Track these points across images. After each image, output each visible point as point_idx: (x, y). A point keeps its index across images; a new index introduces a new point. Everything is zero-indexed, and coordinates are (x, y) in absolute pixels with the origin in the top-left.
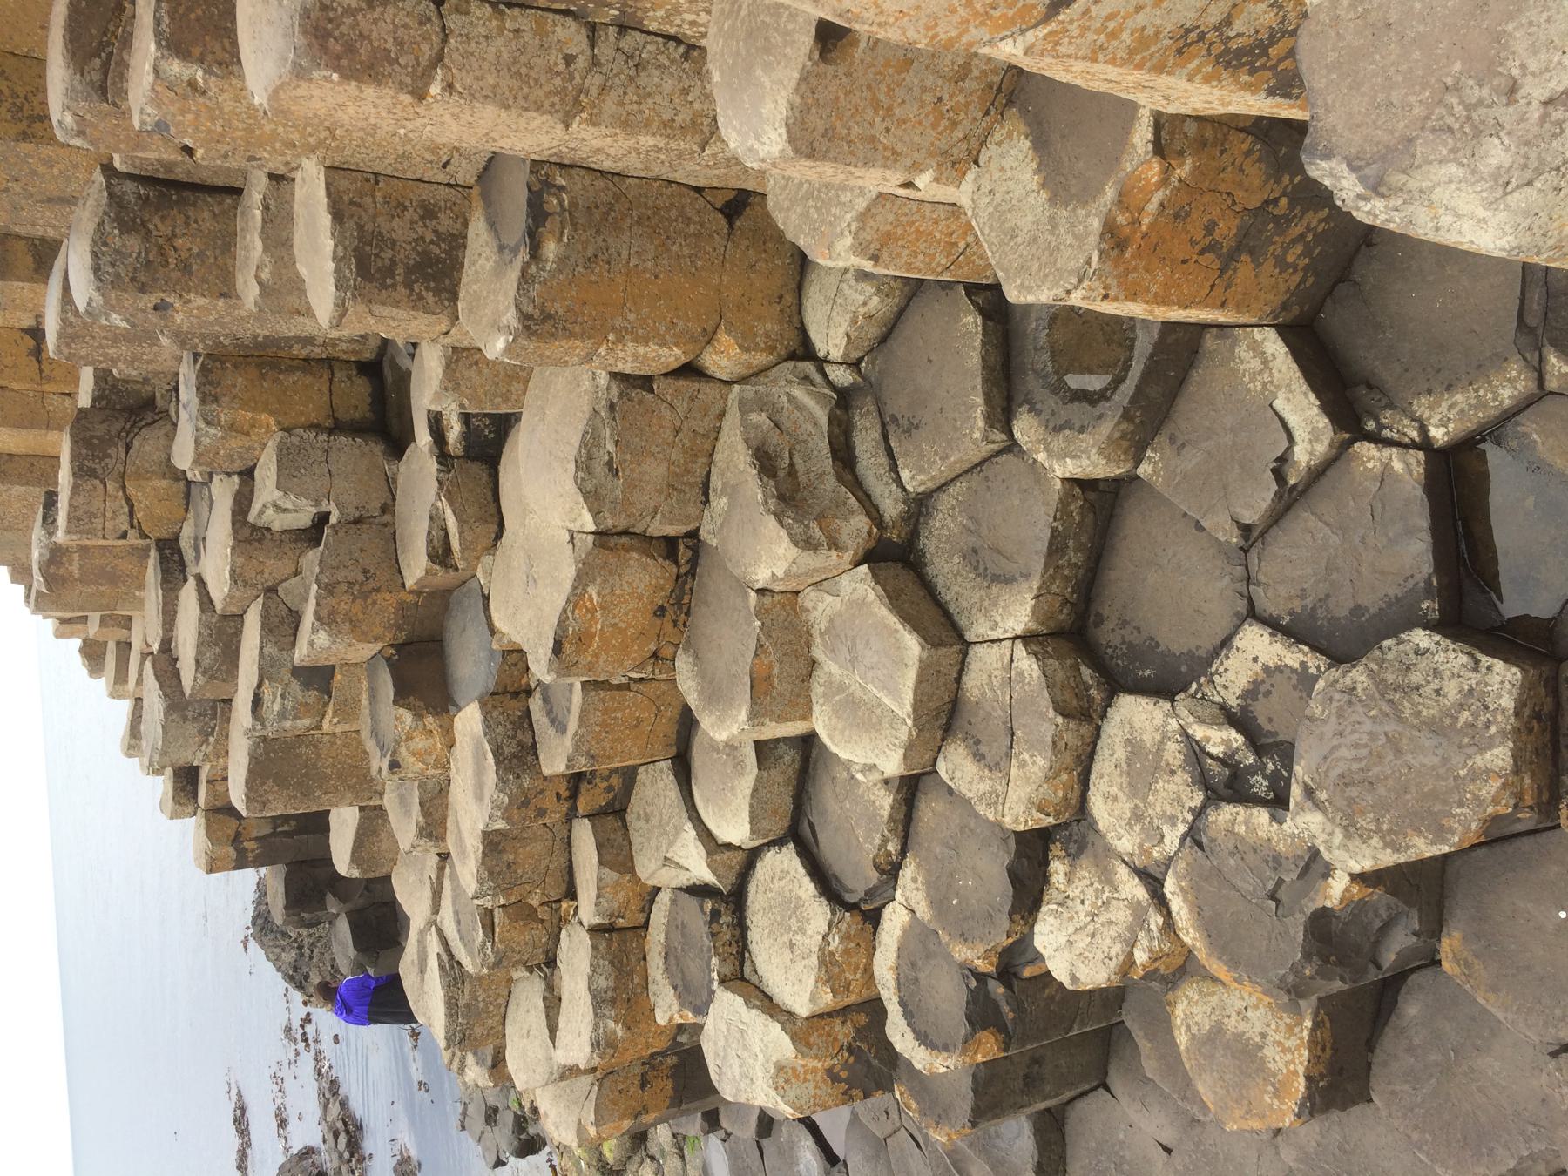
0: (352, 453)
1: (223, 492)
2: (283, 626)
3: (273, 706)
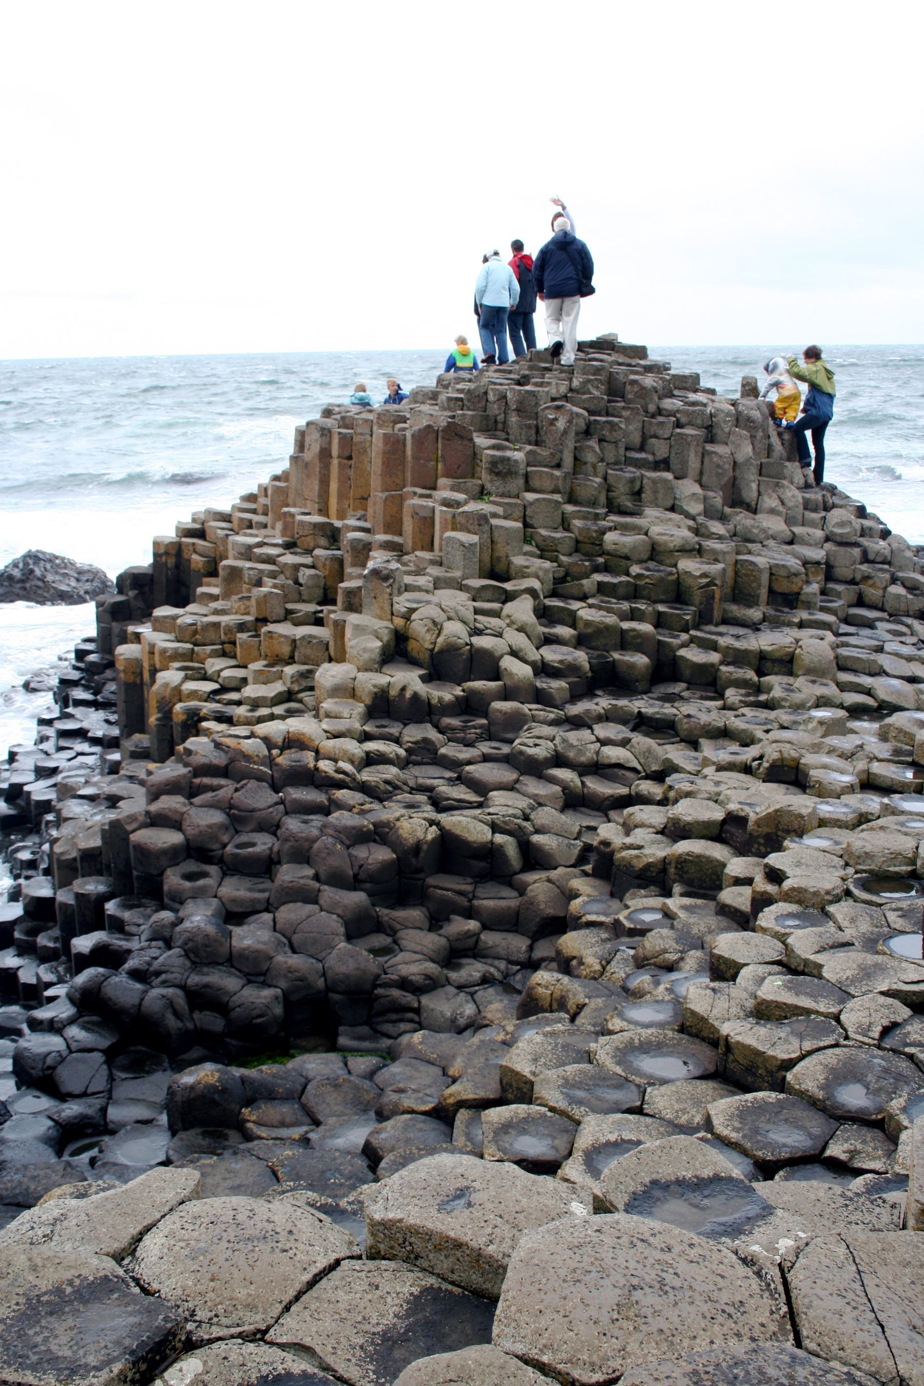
0: (319, 593)
1: (308, 560)
2: (273, 575)
3: (251, 572)
